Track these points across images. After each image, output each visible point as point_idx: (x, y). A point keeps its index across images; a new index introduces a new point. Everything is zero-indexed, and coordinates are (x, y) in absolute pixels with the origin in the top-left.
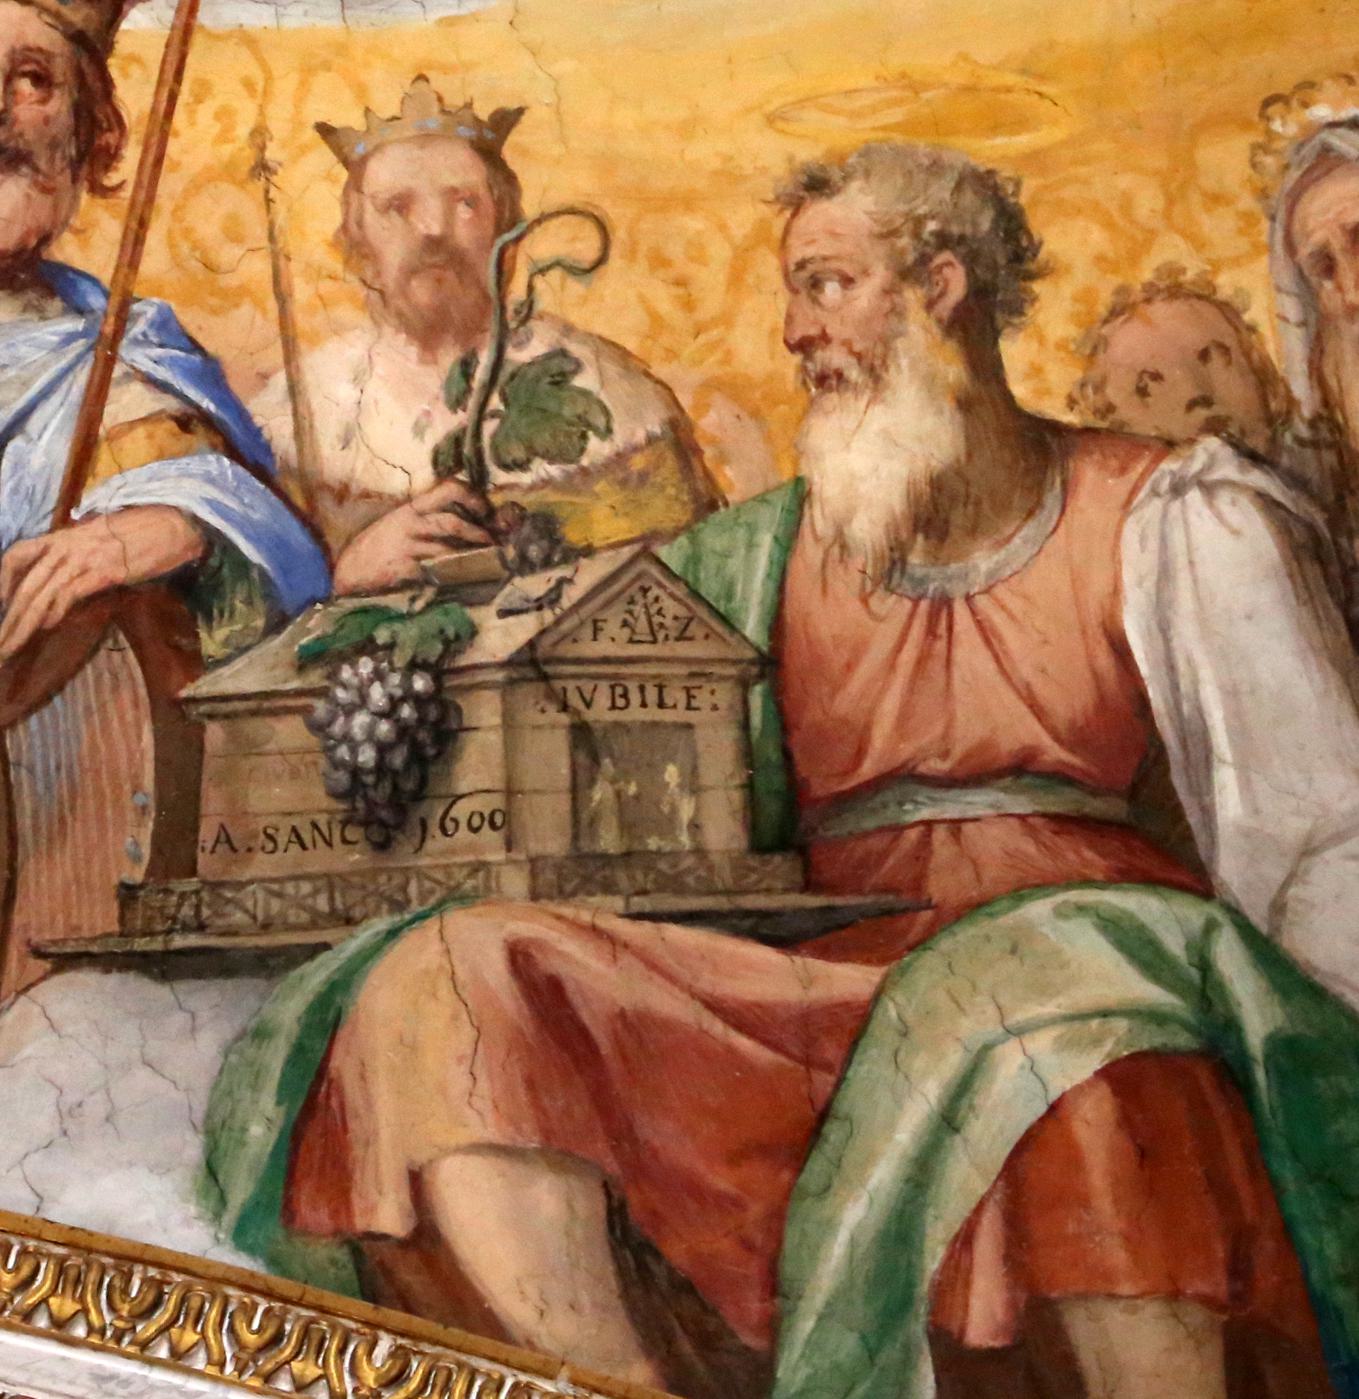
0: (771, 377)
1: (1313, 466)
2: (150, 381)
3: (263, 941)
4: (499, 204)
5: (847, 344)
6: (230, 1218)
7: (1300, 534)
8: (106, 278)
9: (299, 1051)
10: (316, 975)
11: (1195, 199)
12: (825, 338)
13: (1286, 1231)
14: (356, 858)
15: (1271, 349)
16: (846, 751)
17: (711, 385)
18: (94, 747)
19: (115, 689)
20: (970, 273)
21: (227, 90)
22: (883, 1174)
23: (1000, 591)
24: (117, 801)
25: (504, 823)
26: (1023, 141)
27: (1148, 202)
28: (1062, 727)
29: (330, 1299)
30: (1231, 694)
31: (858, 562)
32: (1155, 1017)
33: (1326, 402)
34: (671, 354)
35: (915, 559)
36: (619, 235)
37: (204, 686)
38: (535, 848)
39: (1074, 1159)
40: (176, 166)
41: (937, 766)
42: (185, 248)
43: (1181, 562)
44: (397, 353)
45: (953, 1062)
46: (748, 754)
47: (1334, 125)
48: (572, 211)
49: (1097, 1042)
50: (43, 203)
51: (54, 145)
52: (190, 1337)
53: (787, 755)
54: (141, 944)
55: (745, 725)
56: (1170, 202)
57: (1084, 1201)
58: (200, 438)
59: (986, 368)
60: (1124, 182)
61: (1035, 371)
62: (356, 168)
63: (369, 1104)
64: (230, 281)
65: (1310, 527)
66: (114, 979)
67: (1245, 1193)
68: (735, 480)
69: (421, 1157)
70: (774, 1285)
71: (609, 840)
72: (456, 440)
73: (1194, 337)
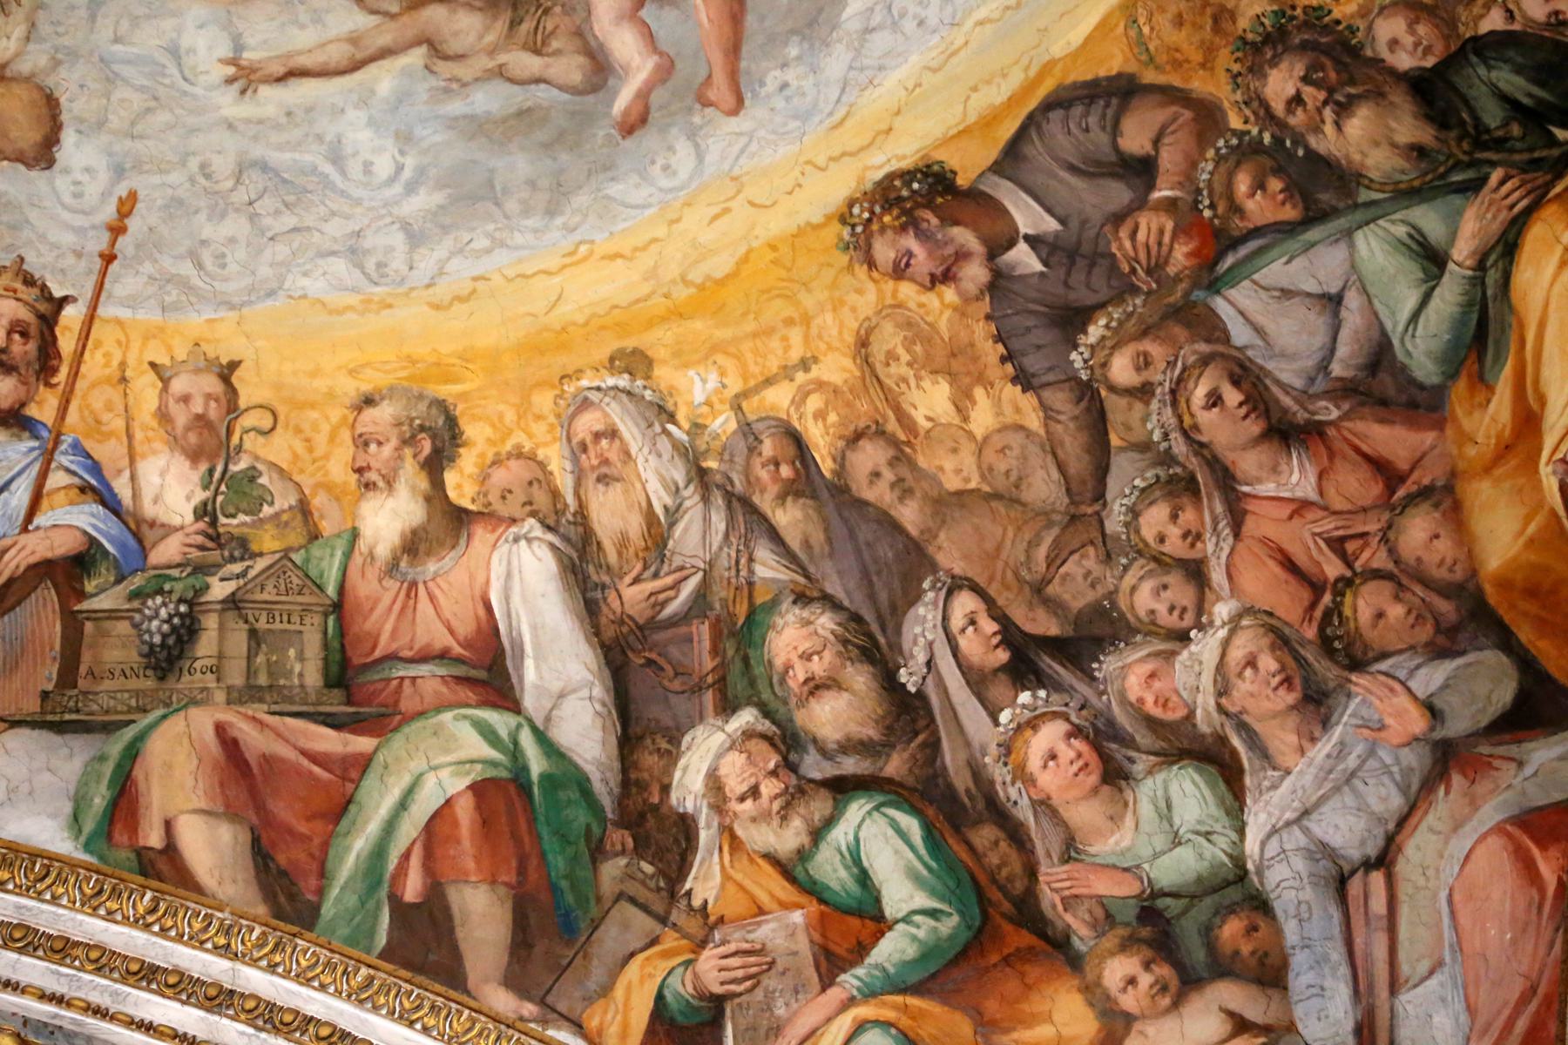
0: (345, 483)
1: (573, 532)
2: (68, 470)
3: (106, 718)
4: (229, 401)
5: (379, 471)
6: (83, 839)
7: (566, 561)
8: (50, 423)
9: (119, 766)
10: (129, 733)
11: (530, 417)
12: (369, 468)
13: (542, 856)
14: (150, 683)
15: (558, 482)
16: (369, 645)
17: (318, 486)
18: (33, 632)
19: (45, 605)
20: (433, 443)
21: (109, 345)
22: (373, 827)
23: (438, 580)
24: (43, 652)
25: (217, 671)
26: (457, 388)
27: (510, 416)
28: (461, 638)
29: (125, 875)
30: (534, 628)
31: (378, 564)
32: (493, 764)
33: (581, 506)
34: (302, 471)
35: (403, 564)
36: (281, 418)
37: (86, 605)
38: (230, 682)
39: (455, 824)
40: (84, 376)
41: (407, 653)
42: (86, 413)
43: (516, 572)
44: (180, 464)
45: (406, 780)
46: (326, 645)
47: (590, 388)
48: (261, 407)
49: (468, 773)
50: (22, 389)
51: (28, 364)
52: (61, 890)
53: (343, 646)
54: (50, 718)
55: (325, 633)
56: (520, 417)
57: (458, 842)
58: (89, 496)
59: (438, 484)
60: (501, 407)
61: (459, 486)
62: (166, 382)
63: (149, 789)
64: (104, 428)
65: (571, 559)
66: (36, 733)
67: (526, 839)
68: (327, 527)
69: (170, 815)
70: (323, 874)
71: (262, 680)
72: (205, 504)
73: (527, 476)
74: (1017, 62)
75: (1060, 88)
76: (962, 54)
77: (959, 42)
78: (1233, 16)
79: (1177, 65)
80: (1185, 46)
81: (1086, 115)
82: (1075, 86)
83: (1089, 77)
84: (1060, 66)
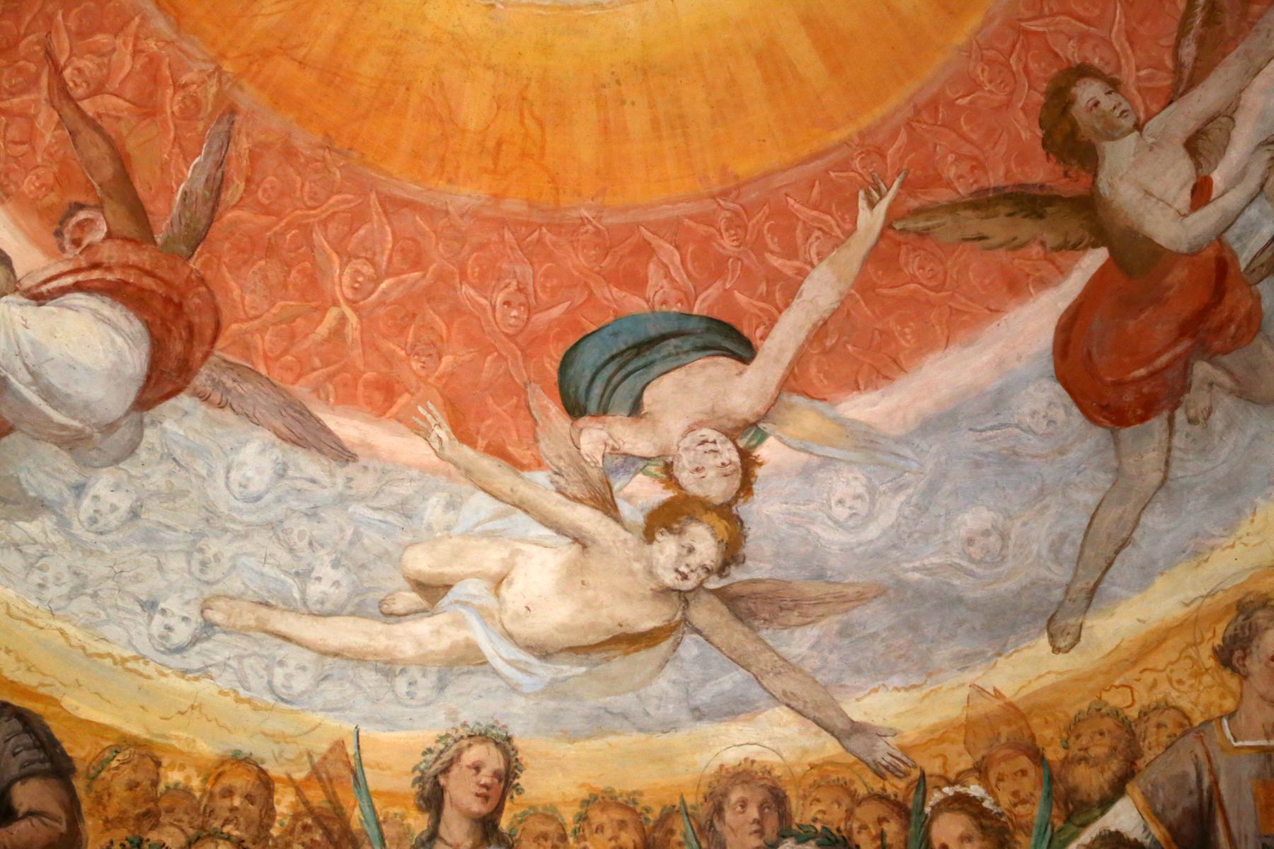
74: (44, 675)
75: (38, 718)
76: (31, 629)
77: (40, 623)
78: (156, 825)
79: (98, 800)
80: (115, 800)
81: (27, 748)
82: (46, 728)
83: (58, 736)
84: (57, 709)
